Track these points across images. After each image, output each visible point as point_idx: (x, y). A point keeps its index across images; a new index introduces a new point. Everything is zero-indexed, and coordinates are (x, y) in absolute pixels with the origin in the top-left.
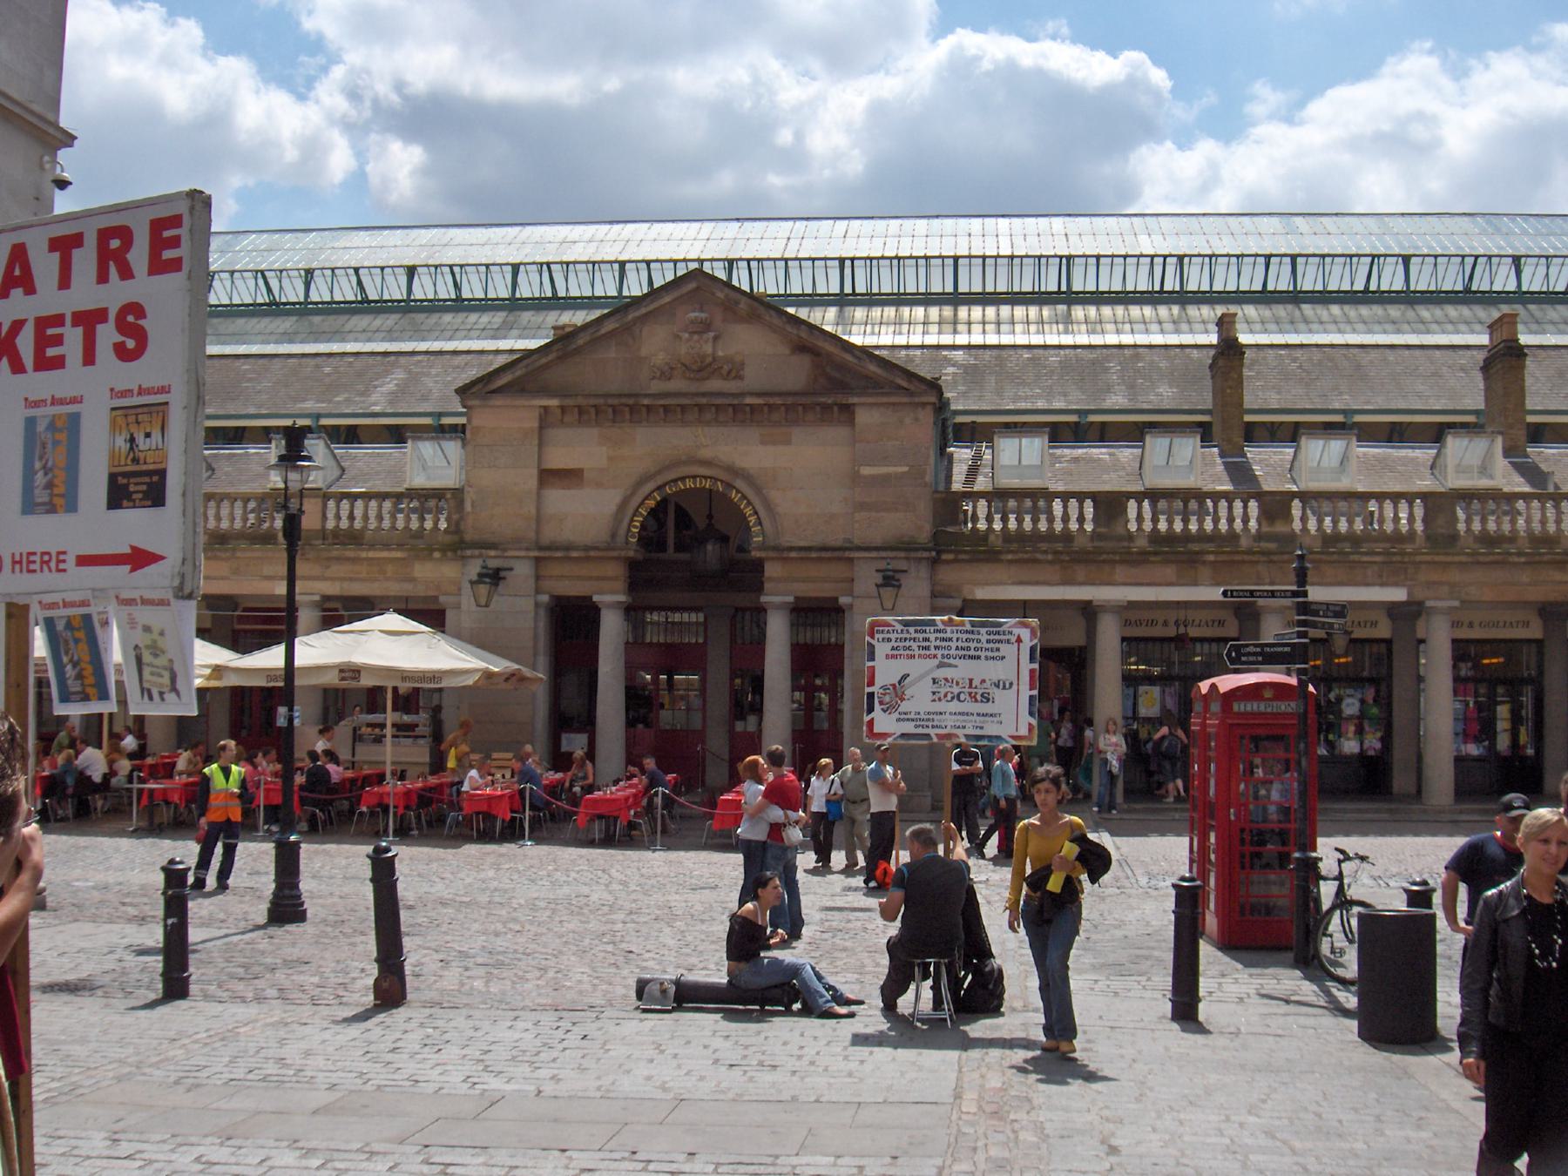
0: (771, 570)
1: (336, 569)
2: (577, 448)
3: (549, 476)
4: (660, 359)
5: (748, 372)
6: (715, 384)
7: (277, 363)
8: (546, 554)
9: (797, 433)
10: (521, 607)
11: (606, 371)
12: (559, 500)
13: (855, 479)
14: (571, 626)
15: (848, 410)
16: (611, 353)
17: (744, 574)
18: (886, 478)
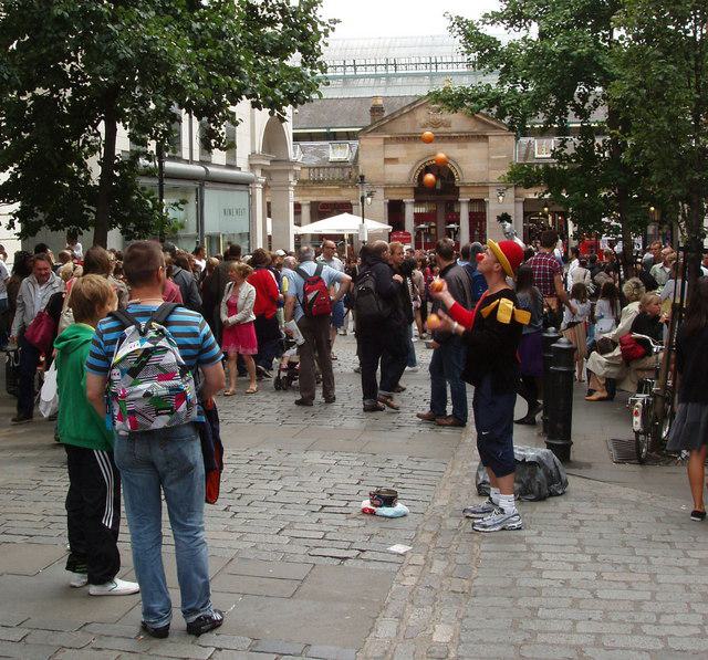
0: (461, 190)
1: (315, 193)
2: (396, 151)
3: (388, 160)
4: (423, 121)
5: (453, 124)
6: (442, 129)
7: (305, 126)
8: (387, 188)
9: (469, 144)
10: (378, 204)
11: (405, 126)
12: (390, 168)
13: (489, 159)
14: (395, 212)
15: (487, 137)
16: (407, 119)
17: (455, 191)
18: (499, 159)
